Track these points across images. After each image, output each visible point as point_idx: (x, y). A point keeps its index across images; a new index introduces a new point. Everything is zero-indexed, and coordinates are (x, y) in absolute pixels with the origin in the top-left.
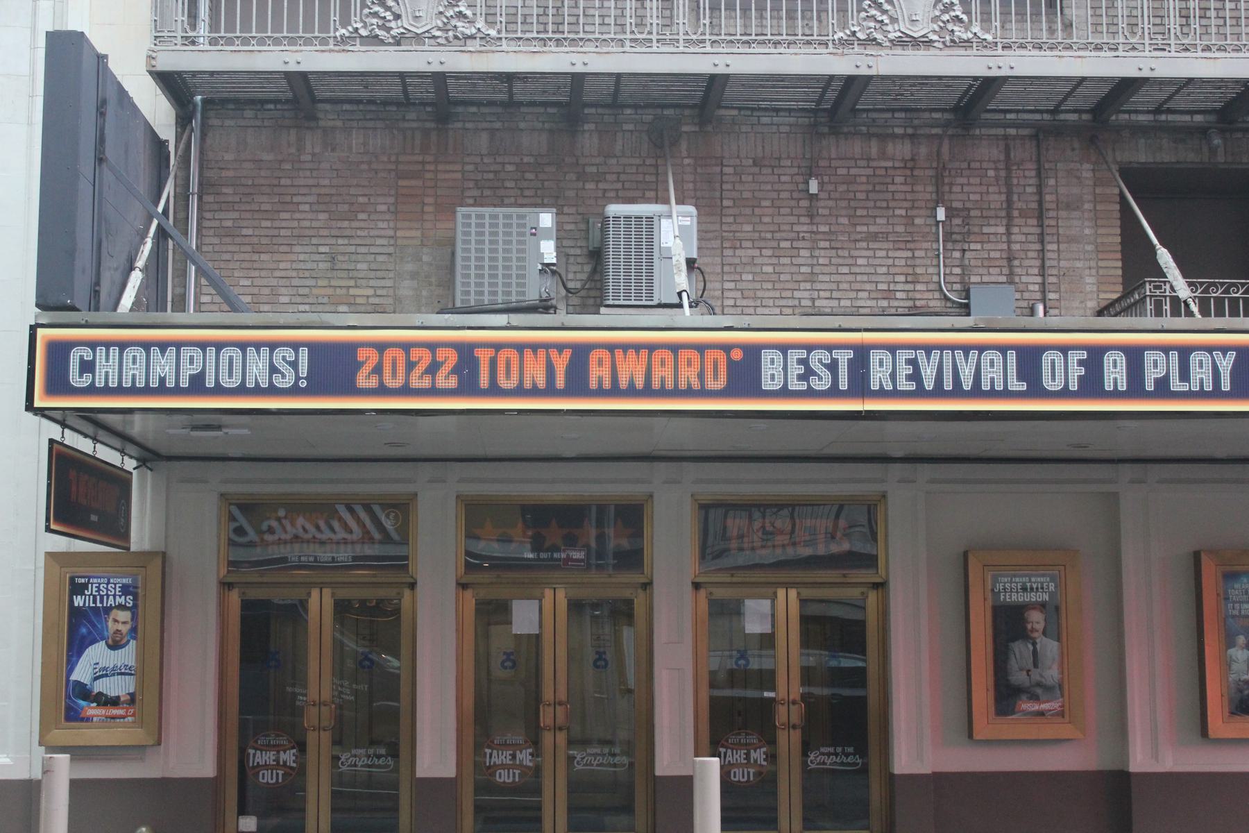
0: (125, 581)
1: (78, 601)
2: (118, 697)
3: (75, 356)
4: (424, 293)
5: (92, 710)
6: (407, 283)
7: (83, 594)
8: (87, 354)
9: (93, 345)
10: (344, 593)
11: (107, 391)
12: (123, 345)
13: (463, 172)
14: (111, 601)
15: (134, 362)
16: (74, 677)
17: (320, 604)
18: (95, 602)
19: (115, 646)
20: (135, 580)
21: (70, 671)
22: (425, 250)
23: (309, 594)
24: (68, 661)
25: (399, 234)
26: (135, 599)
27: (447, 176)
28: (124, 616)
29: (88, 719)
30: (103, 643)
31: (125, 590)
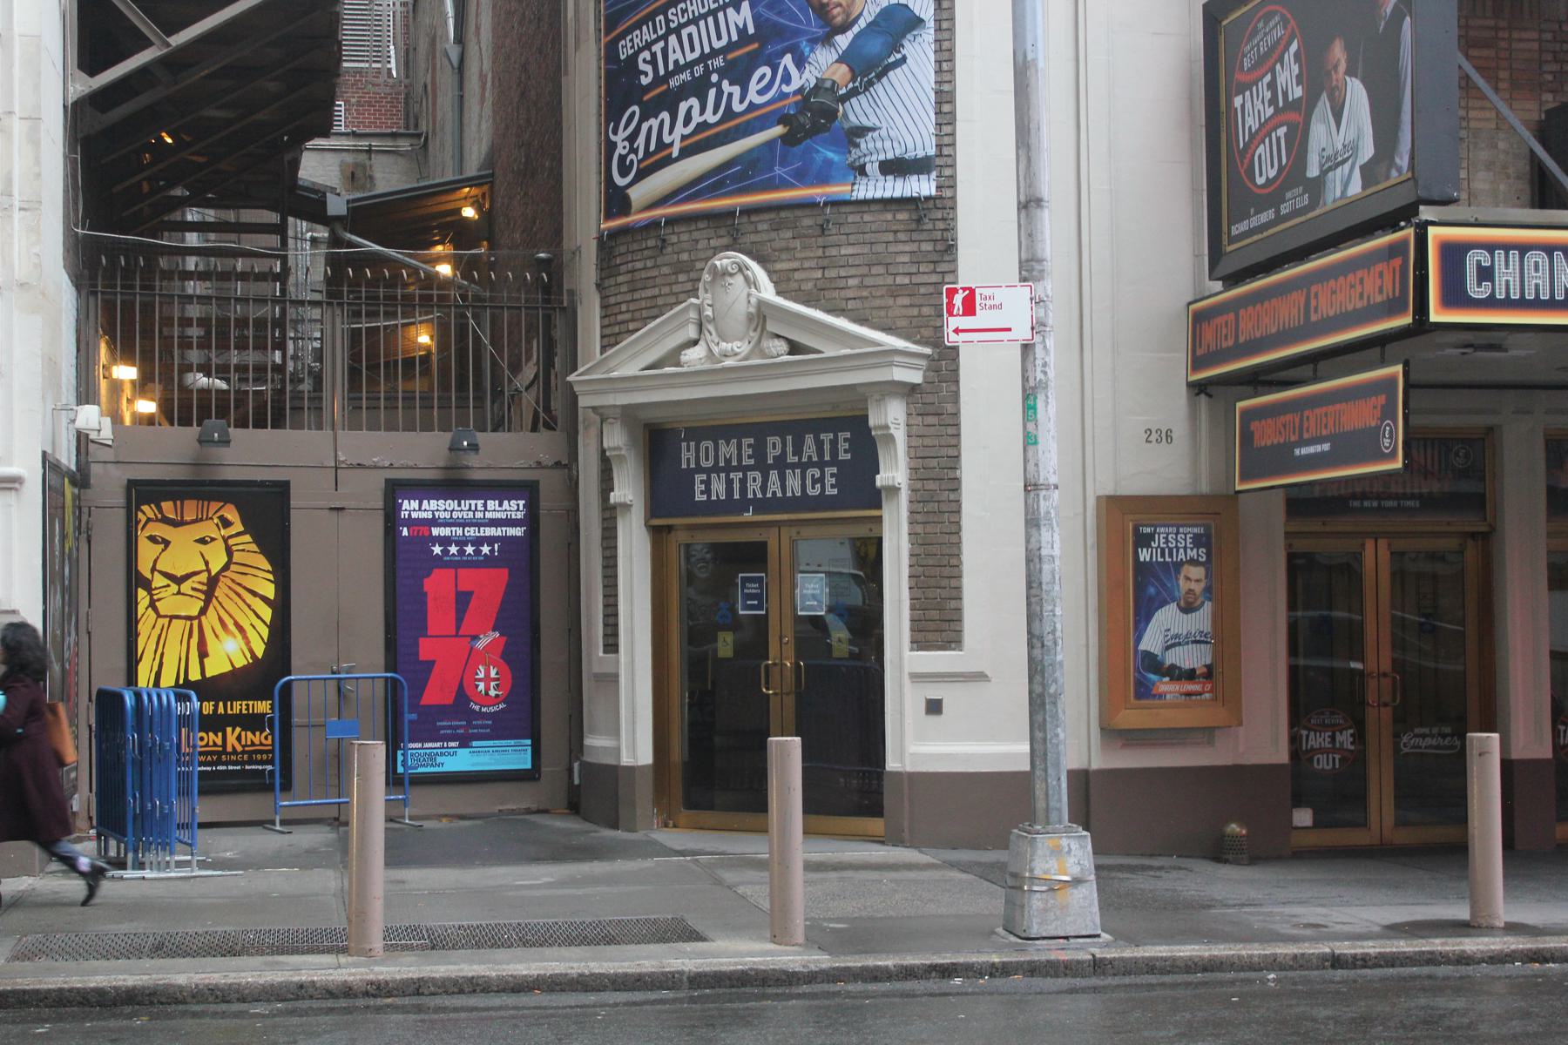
0: (1196, 530)
1: (1144, 555)
2: (1194, 670)
3: (1474, 258)
4: (1502, 187)
5: (1165, 686)
6: (1482, 175)
7: (1149, 546)
8: (1482, 257)
9: (1490, 247)
10: (1401, 545)
11: (1508, 304)
12: (1524, 248)
13: (1540, 40)
14: (1181, 556)
15: (1537, 270)
16: (1142, 647)
17: (1376, 559)
18: (1163, 555)
19: (1188, 609)
20: (1207, 528)
21: (1138, 640)
22: (1502, 135)
23: (1363, 545)
24: (1137, 623)
25: (1472, 114)
26: (1208, 554)
27: (1521, 45)
28: (1197, 572)
29: (1161, 696)
30: (1173, 606)
31: (1198, 541)
